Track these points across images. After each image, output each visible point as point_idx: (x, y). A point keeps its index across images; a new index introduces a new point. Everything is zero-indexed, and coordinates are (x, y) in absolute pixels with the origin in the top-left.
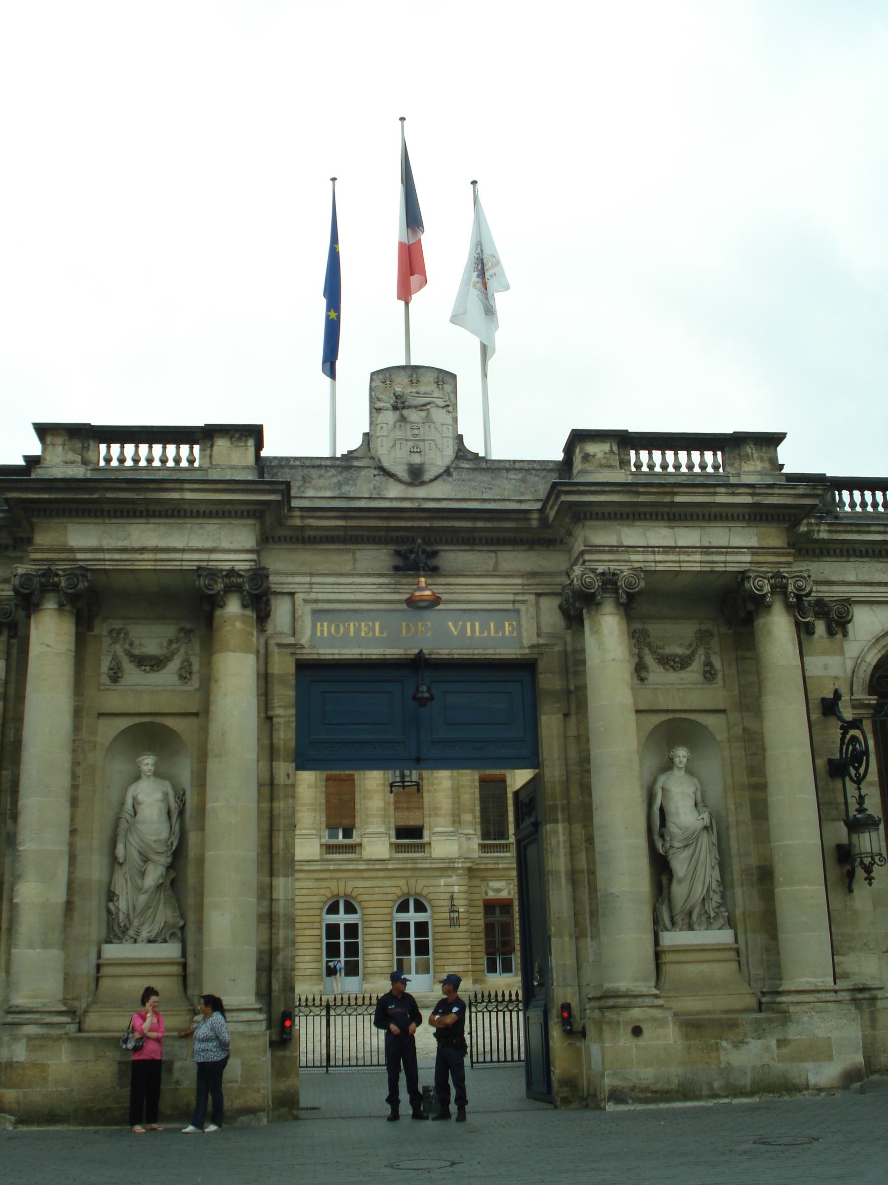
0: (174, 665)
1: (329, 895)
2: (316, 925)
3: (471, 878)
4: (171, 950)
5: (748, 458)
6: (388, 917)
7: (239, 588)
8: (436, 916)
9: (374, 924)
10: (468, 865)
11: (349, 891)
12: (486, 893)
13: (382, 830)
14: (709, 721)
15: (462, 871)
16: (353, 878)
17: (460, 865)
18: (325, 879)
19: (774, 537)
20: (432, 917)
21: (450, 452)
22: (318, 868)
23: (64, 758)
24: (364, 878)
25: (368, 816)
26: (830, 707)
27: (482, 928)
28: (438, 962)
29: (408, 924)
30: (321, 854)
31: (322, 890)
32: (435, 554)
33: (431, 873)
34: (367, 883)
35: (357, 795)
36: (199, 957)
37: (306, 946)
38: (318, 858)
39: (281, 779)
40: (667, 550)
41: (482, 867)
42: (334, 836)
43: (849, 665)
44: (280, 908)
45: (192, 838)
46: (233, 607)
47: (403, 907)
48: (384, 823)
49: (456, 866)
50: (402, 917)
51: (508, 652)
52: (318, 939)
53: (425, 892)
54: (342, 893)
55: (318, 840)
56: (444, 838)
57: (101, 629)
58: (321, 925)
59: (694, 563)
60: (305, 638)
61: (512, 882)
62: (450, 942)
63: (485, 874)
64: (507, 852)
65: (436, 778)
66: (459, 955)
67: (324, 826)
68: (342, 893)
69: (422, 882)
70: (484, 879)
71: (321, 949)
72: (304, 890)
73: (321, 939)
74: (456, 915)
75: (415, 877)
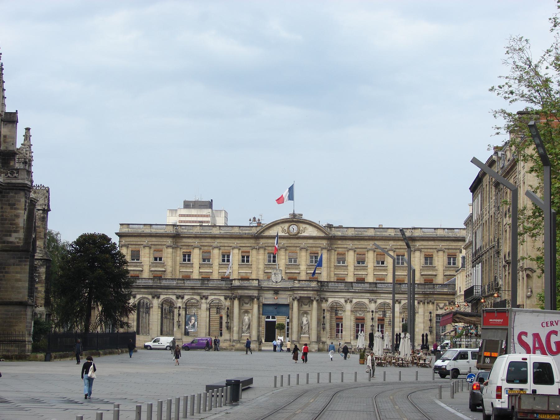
0: (249, 303)
4: (249, 335)
5: (313, 283)
7: (256, 298)
14: (309, 312)
19: (315, 293)
21: (280, 279)
23: (238, 315)
26: (324, 310)
32: (278, 292)
36: (252, 335)
39: (260, 317)
40: (303, 294)
43: (327, 305)
44: (260, 331)
45: (251, 323)
46: (255, 300)
51: (286, 303)
57: (241, 299)
59: (306, 295)
60: (264, 301)
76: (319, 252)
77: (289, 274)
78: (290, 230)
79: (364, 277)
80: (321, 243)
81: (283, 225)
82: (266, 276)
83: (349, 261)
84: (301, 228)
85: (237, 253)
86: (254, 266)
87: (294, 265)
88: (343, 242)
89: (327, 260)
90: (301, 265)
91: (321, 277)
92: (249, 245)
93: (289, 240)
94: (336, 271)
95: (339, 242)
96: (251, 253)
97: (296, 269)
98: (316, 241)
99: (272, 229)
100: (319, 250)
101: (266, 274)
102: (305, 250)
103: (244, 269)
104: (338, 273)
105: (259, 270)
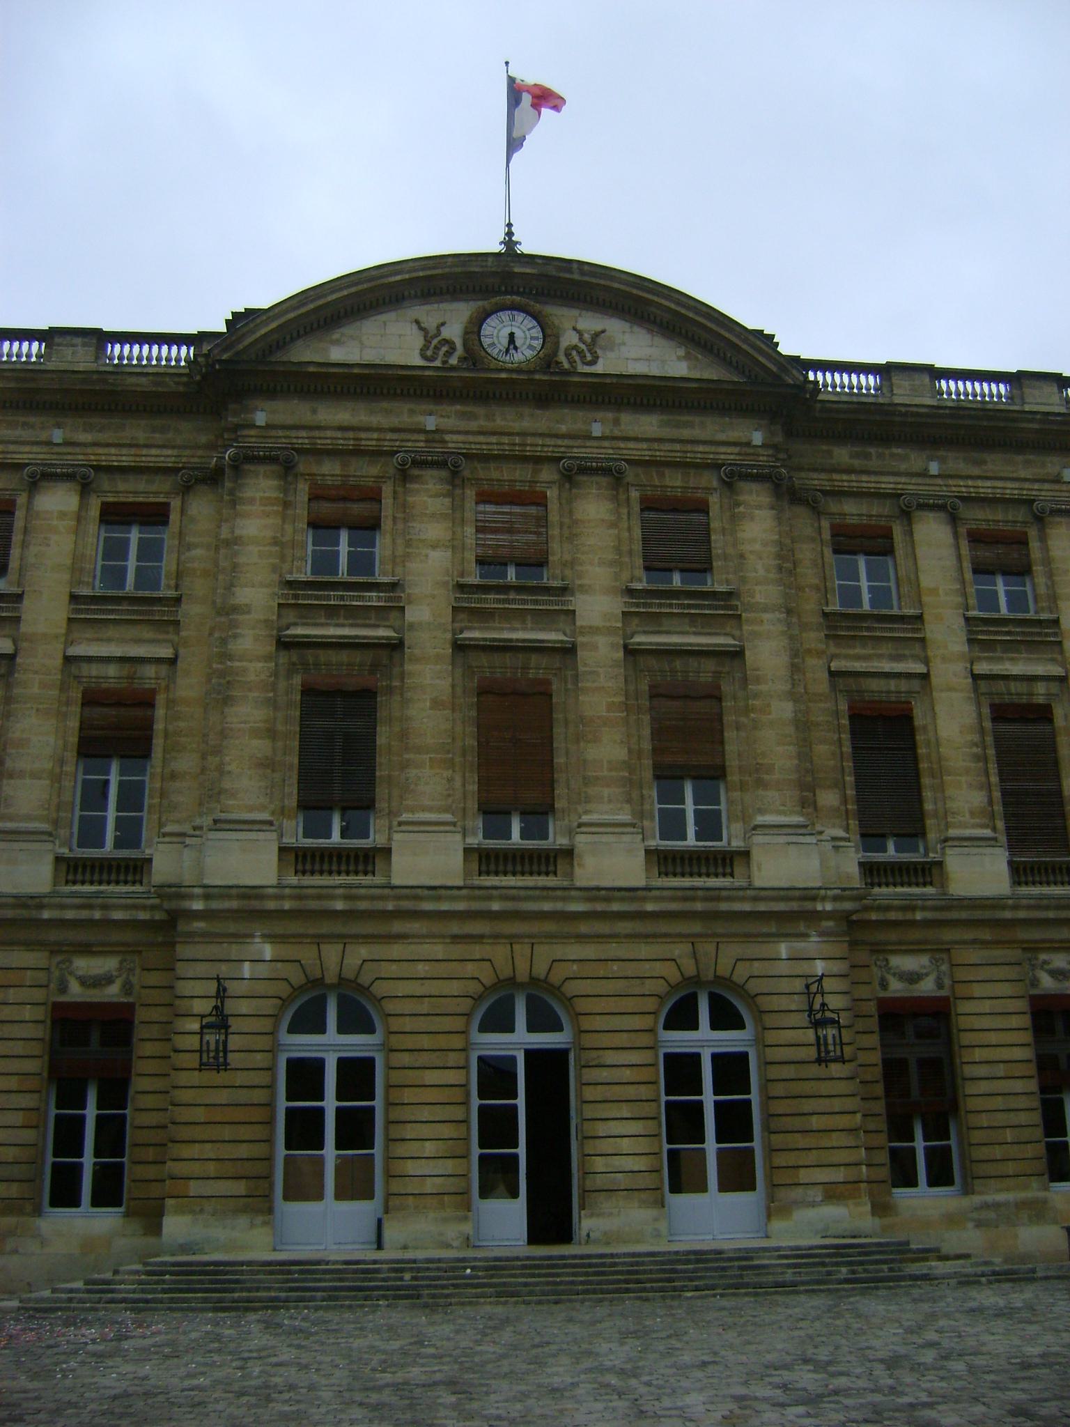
1: (488, 978)
2: (453, 1059)
3: (853, 944)
6: (645, 1039)
8: (771, 1037)
9: (611, 1057)
10: (848, 906)
11: (540, 970)
12: (884, 985)
13: (625, 817)
15: (831, 924)
16: (551, 937)
17: (829, 907)
18: (478, 938)
20: (760, 1042)
22: (460, 906)
24: (581, 938)
25: (587, 781)
27: (877, 1072)
28: (780, 1160)
29: (695, 1058)
30: (467, 874)
31: (470, 966)
33: (751, 927)
34: (590, 951)
35: (558, 731)
37: (425, 1113)
38: (461, 883)
41: (874, 916)
42: (497, 829)
47: (682, 1017)
48: (629, 801)
49: (819, 907)
50: (679, 1041)
52: (457, 1095)
53: (740, 974)
54: (522, 976)
55: (458, 837)
56: (782, 839)
58: (467, 1059)
61: (945, 956)
62: (808, 1106)
63: (880, 936)
64: (925, 885)
65: (756, 696)
66: (836, 1139)
67: (473, 805)
68: (522, 976)
69: (731, 951)
70: (879, 949)
71: (466, 1121)
72: (420, 966)
73: (468, 1094)
74: (831, 1032)
75: (714, 935)
76: (714, 500)
77: (483, 660)
78: (486, 342)
79: (1041, 700)
80: (721, 437)
81: (430, 314)
82: (290, 674)
83: (926, 581)
84: (569, 339)
85: (62, 515)
86: (192, 611)
87: (519, 589)
88: (867, 456)
89: (779, 556)
90: (584, 589)
91: (745, 681)
92: (166, 457)
93: (480, 411)
94: (833, 657)
95: (842, 454)
96: (174, 517)
97: (545, 618)
98: (690, 425)
99: (348, 330)
100: (709, 490)
101: (294, 656)
102: (604, 480)
103: (111, 632)
104: (859, 666)
105: (233, 625)
